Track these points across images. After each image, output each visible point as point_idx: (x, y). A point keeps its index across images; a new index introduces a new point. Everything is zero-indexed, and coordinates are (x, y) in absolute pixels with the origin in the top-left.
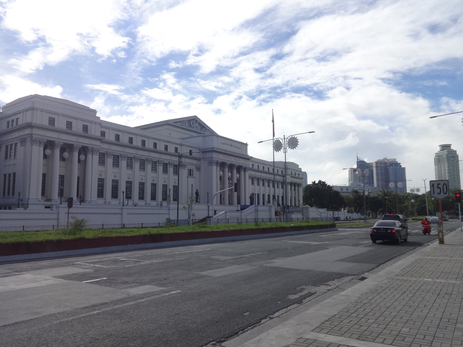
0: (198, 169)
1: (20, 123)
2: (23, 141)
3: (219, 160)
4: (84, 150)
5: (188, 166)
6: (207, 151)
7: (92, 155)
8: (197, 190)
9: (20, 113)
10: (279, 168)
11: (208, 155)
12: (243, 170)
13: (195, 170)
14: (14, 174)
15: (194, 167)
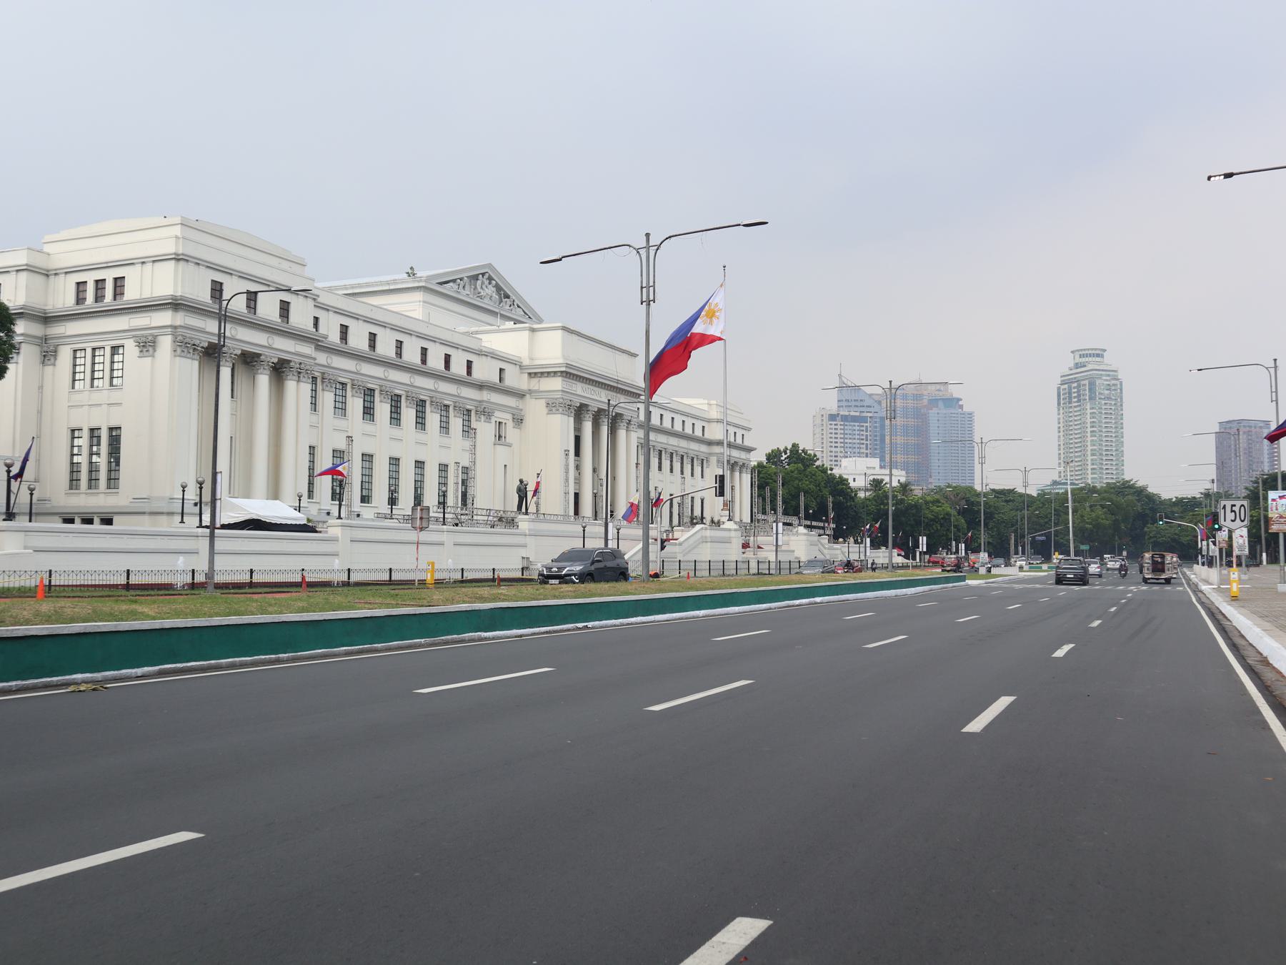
0: (519, 421)
1: (132, 293)
2: (147, 345)
4: (280, 370)
12: (623, 425)
13: (510, 424)
15: (509, 417)
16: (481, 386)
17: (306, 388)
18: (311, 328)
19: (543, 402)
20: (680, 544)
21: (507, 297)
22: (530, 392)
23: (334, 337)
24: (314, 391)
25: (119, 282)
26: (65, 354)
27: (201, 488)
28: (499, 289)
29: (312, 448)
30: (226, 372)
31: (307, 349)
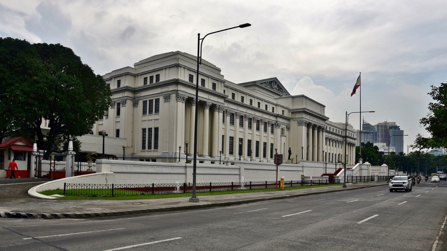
0: (288, 128)
1: (162, 80)
2: (167, 98)
3: (307, 120)
4: (213, 108)
5: (282, 126)
6: (296, 112)
7: (219, 112)
8: (290, 148)
9: (162, 69)
10: (340, 129)
11: (298, 116)
12: (321, 130)
13: (286, 129)
14: (157, 129)
15: (285, 127)
16: (277, 116)
17: (221, 114)
18: (222, 92)
19: (296, 122)
20: (352, 170)
21: (281, 89)
22: (292, 118)
23: (230, 97)
24: (224, 116)
25: (158, 76)
26: (141, 103)
27: (187, 146)
28: (278, 86)
29: (223, 136)
30: (194, 108)
31: (222, 101)
